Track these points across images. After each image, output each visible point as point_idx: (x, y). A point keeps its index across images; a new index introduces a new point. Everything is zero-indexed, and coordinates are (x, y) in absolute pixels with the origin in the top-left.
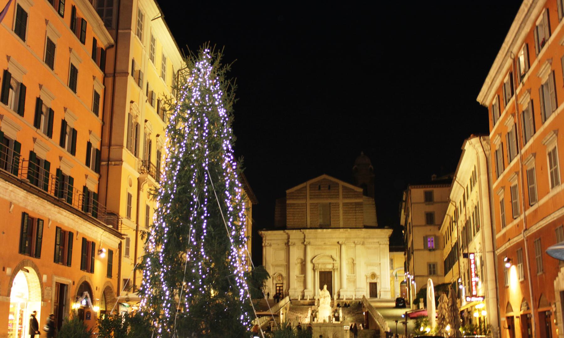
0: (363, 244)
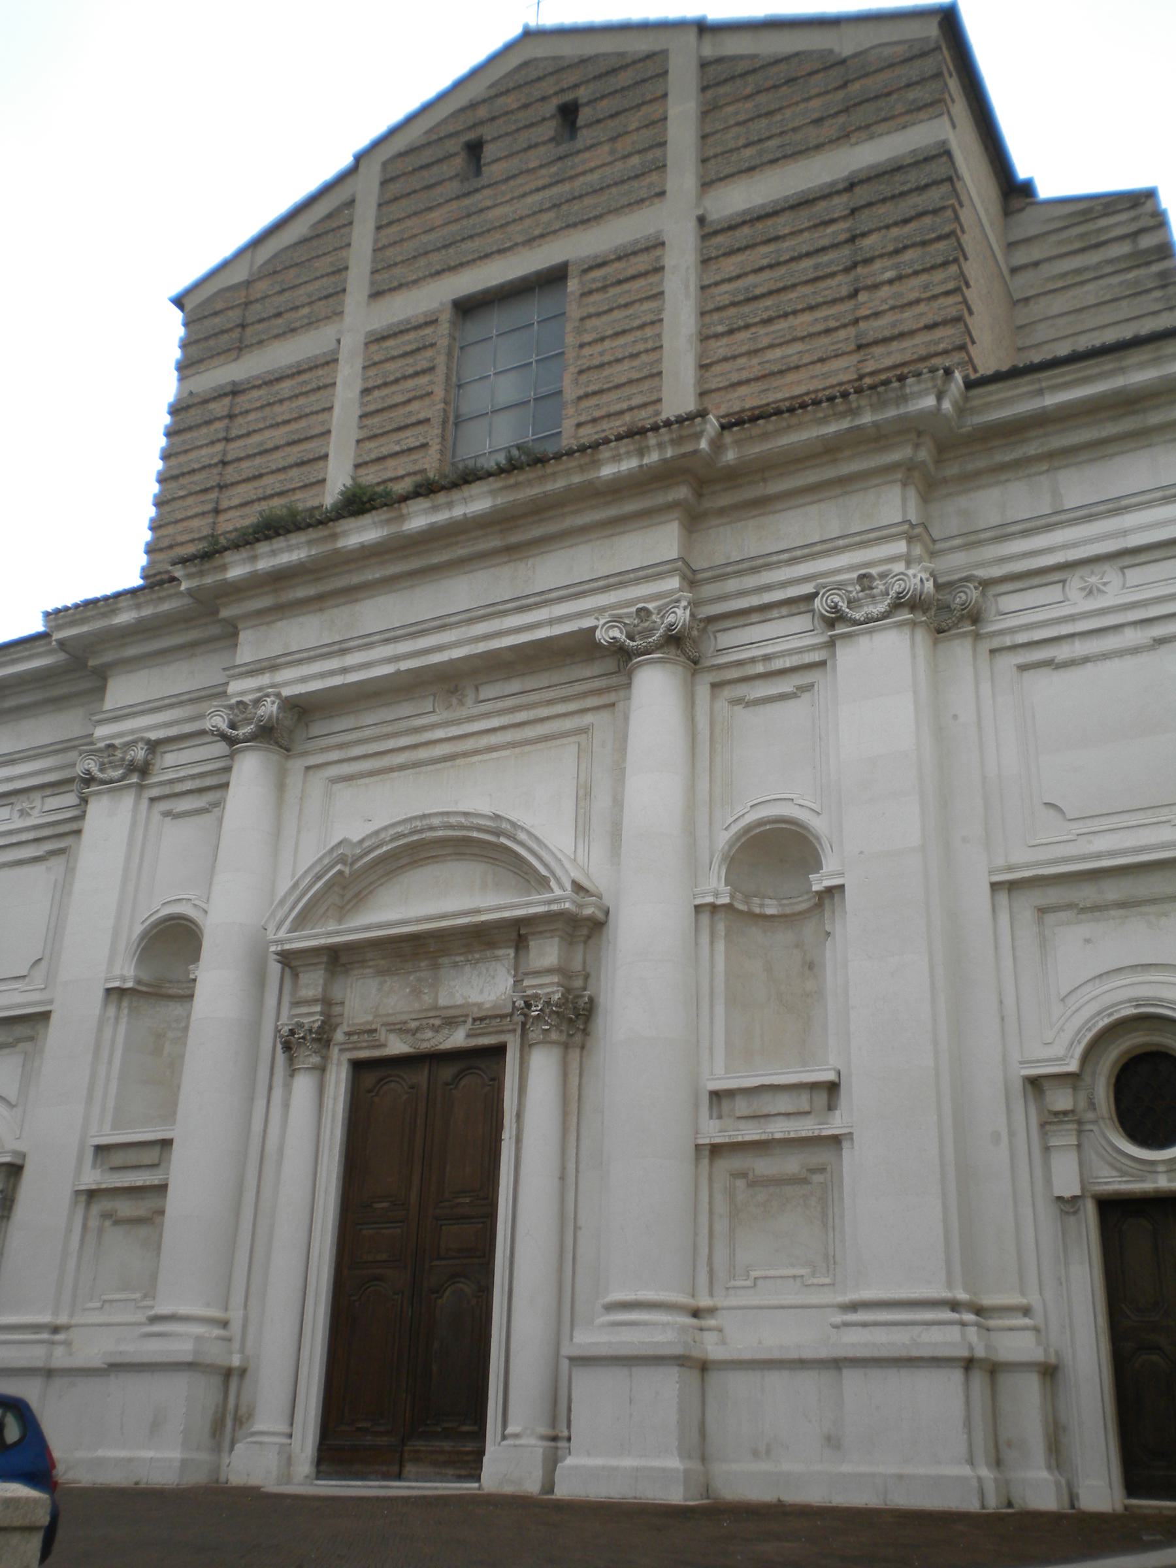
0: (946, 615)
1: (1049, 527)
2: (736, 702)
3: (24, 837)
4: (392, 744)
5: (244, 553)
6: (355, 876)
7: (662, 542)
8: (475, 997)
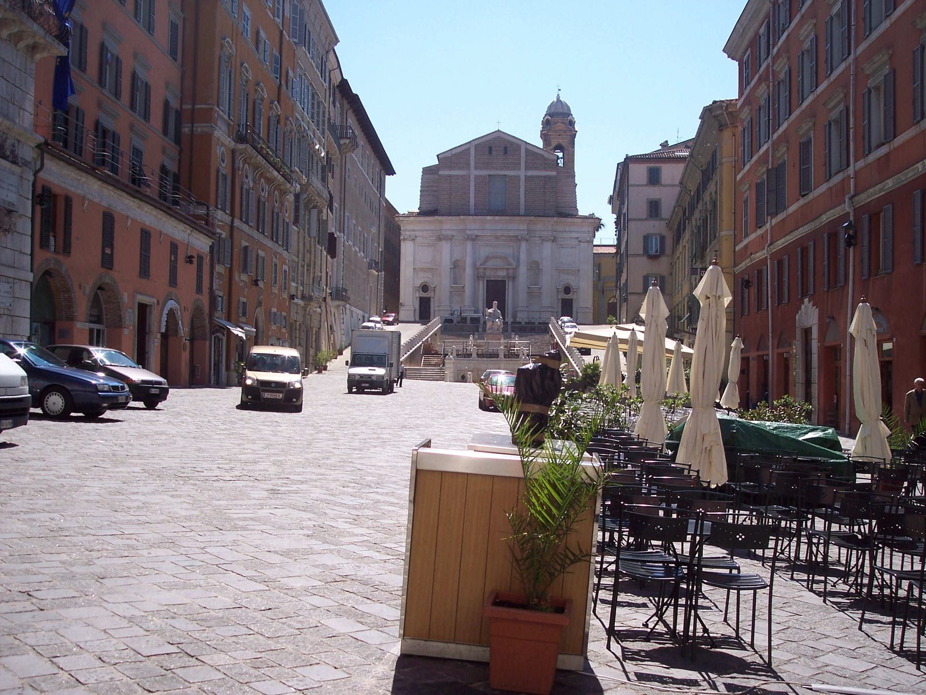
0: (554, 240)
6: (488, 259)
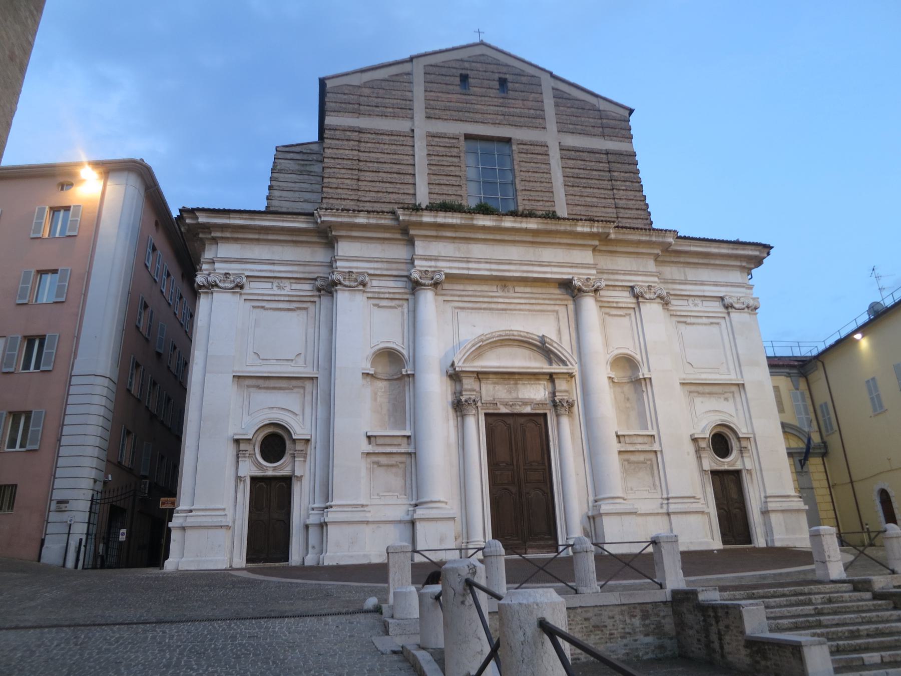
1: (686, 284)
2: (606, 314)
3: (282, 298)
4: (481, 299)
5: (433, 213)
7: (586, 256)
8: (532, 396)
